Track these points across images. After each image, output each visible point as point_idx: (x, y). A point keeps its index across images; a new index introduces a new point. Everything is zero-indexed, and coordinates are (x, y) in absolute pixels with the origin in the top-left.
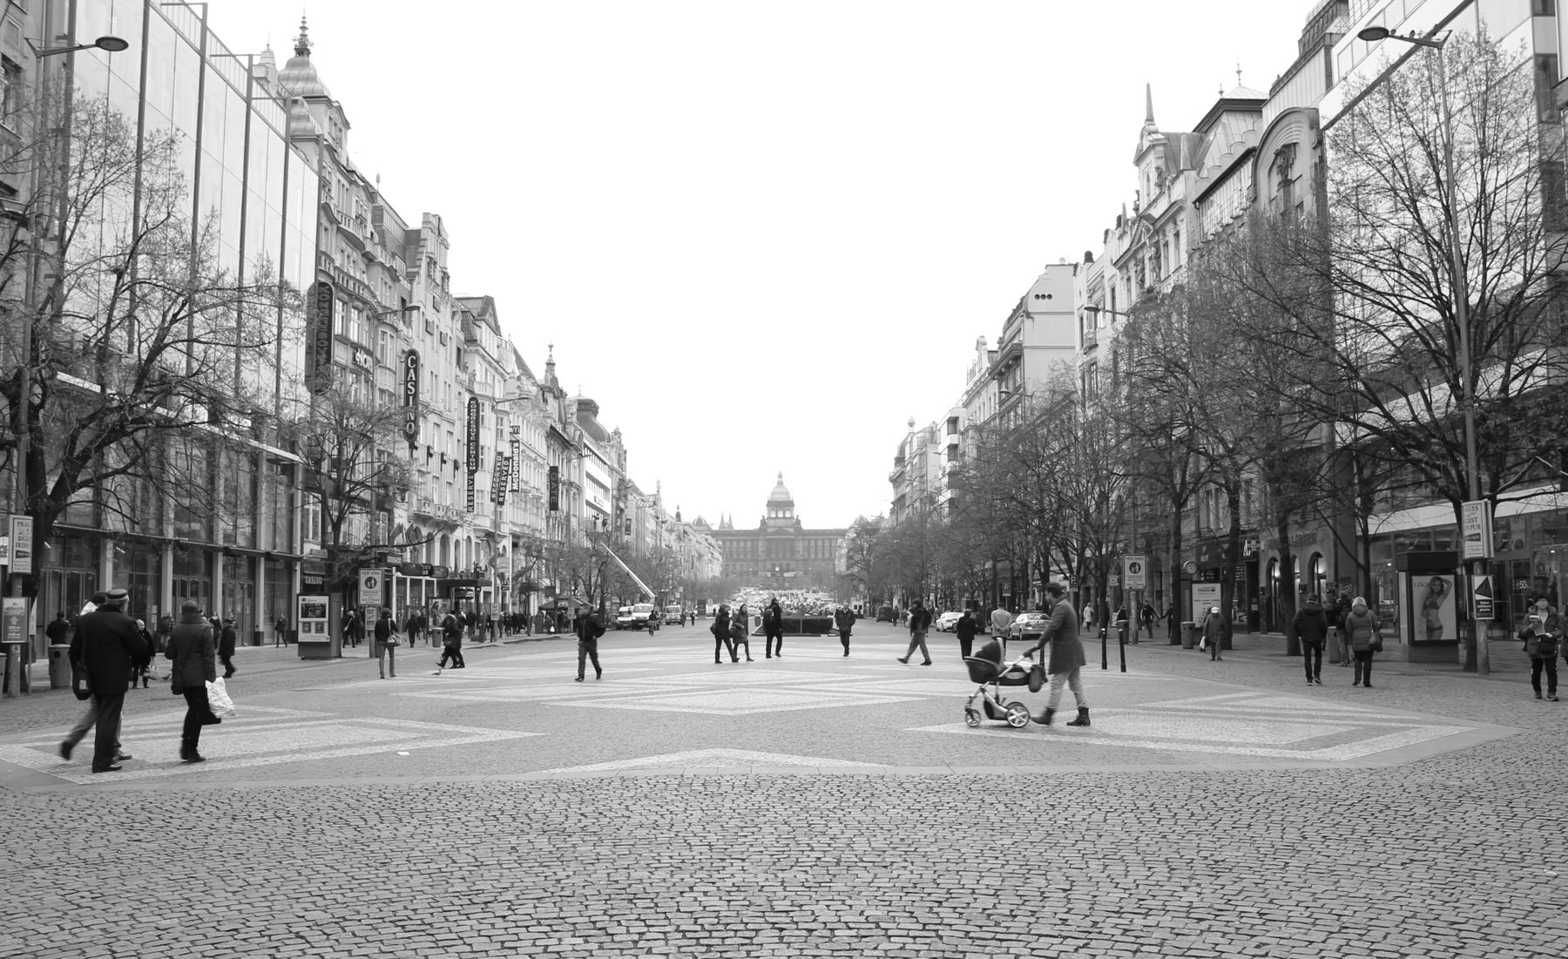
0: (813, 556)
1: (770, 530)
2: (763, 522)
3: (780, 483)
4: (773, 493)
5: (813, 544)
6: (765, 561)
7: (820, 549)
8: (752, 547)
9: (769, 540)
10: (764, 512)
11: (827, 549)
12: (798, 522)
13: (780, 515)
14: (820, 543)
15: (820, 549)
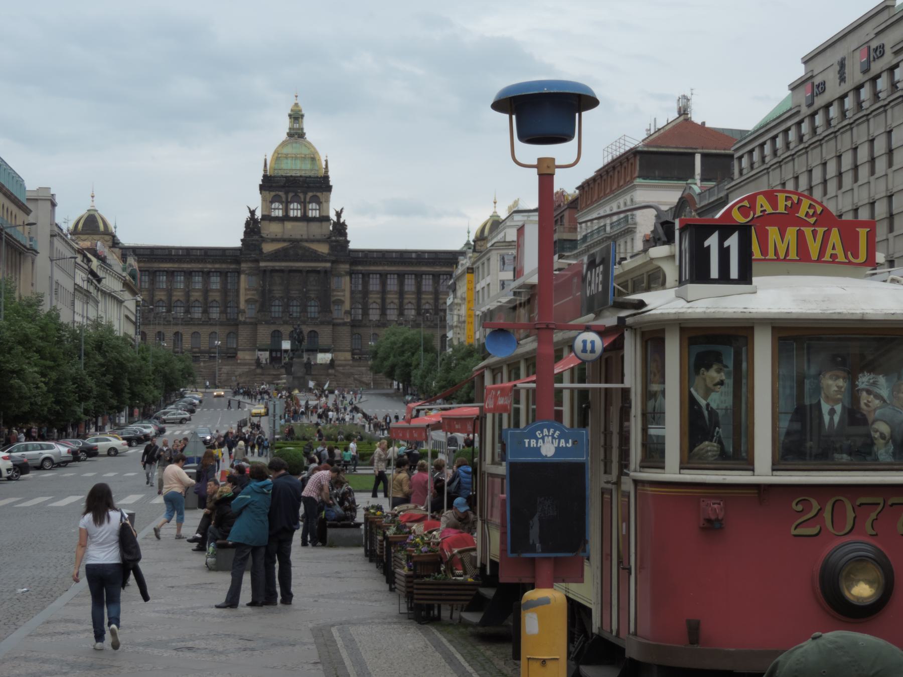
0: (374, 315)
1: (268, 248)
2: (252, 227)
3: (296, 134)
4: (278, 156)
5: (374, 284)
6: (255, 324)
7: (392, 298)
8: (225, 291)
9: (264, 273)
10: (256, 201)
11: (410, 298)
12: (340, 228)
13: (295, 211)
14: (392, 284)
15: (392, 298)
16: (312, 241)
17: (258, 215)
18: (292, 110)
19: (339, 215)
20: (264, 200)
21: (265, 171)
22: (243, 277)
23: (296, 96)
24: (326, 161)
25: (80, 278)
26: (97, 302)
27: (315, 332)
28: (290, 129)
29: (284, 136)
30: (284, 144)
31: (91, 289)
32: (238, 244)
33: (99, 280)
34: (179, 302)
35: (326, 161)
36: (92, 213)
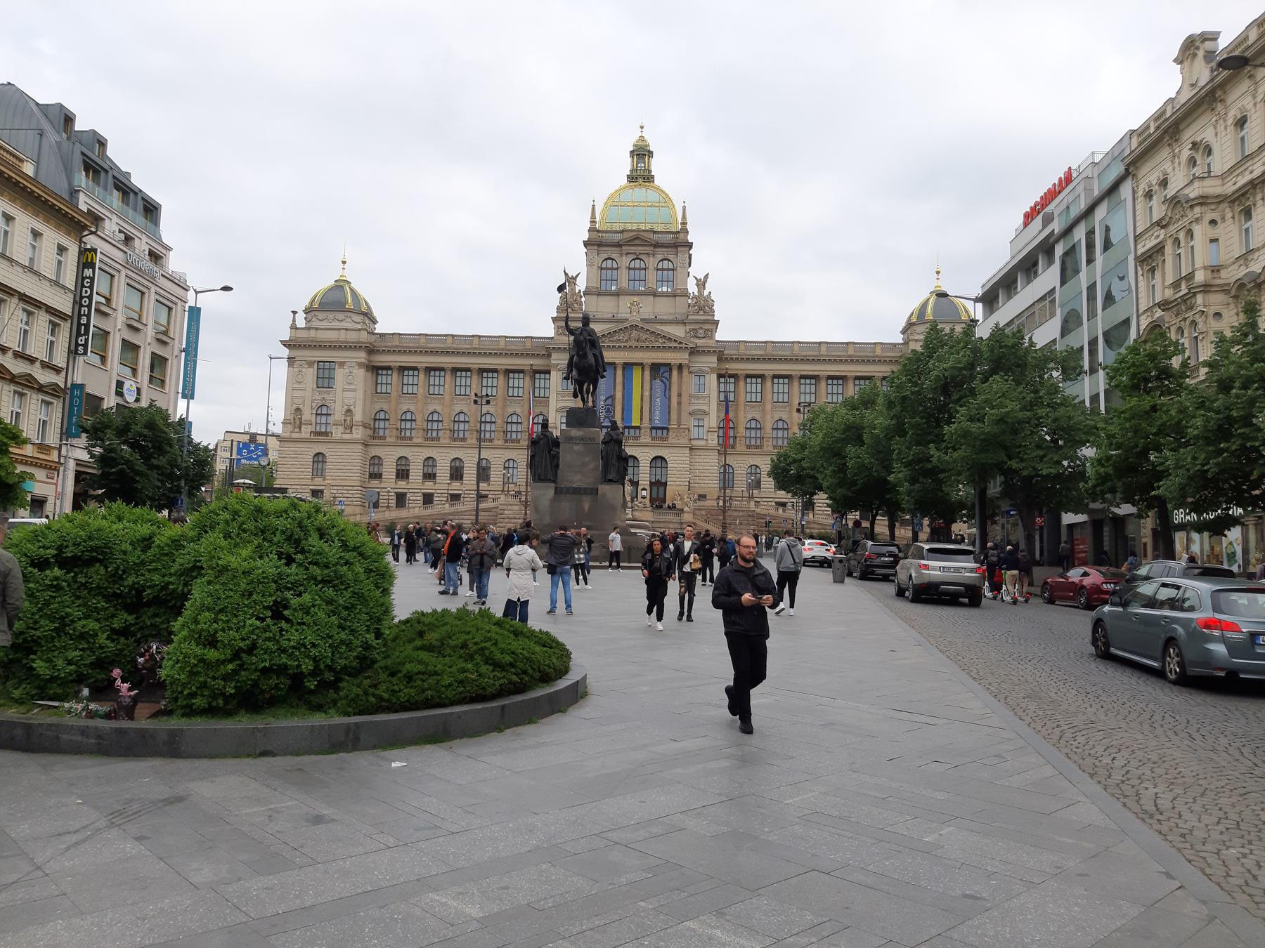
3: (641, 176)
12: (704, 306)
16: (663, 322)
17: (581, 285)
18: (635, 145)
19: (701, 284)
21: (593, 222)
23: (642, 127)
24: (684, 208)
27: (662, 458)
28: (632, 171)
29: (624, 181)
30: (622, 189)
34: (462, 415)
35: (684, 208)
36: (342, 283)
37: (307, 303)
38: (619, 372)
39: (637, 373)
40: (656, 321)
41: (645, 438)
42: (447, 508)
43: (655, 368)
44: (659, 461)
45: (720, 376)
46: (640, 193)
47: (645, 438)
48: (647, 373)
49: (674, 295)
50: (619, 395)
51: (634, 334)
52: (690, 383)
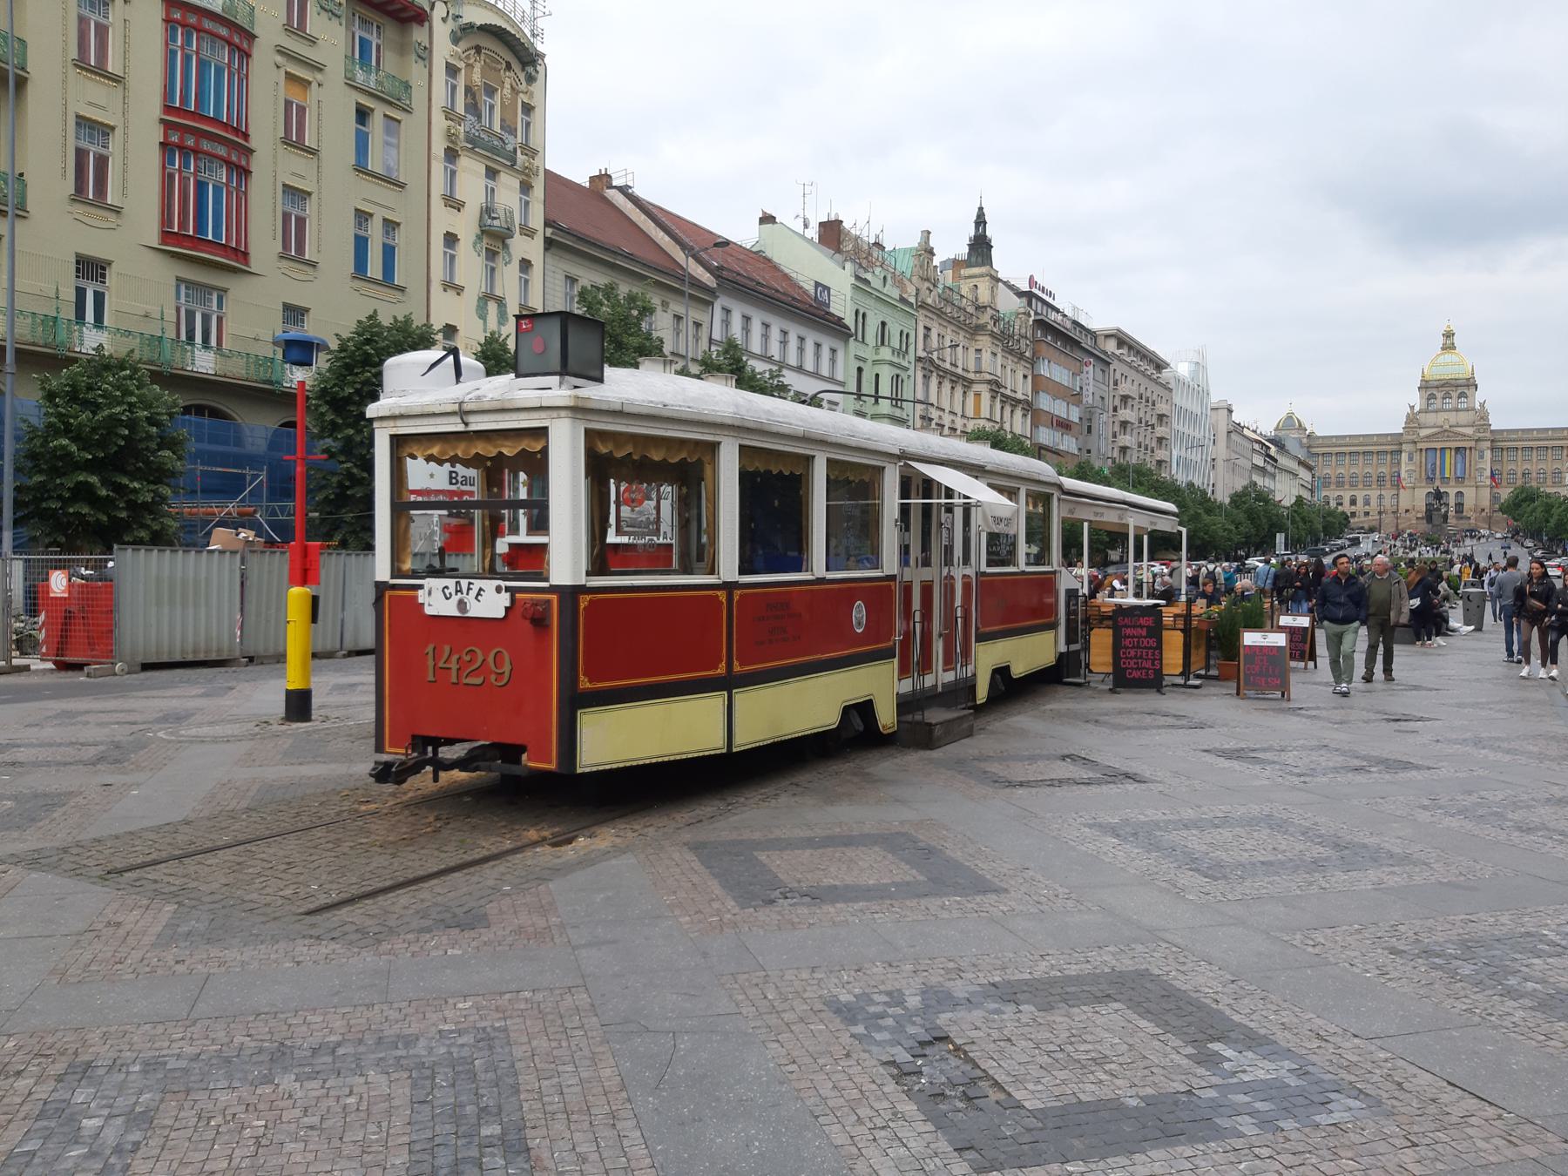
1: (1424, 433)
2: (1412, 420)
3: (1449, 347)
10: (1416, 399)
12: (1483, 416)
19: (1482, 405)
20: (1421, 398)
22: (1403, 454)
25: (1259, 461)
26: (1273, 476)
29: (1439, 351)
31: (1269, 468)
32: (1401, 431)
33: (1276, 461)
37: (1275, 425)
38: (1438, 452)
39: (1448, 452)
40: (1458, 426)
41: (1452, 483)
42: (1363, 519)
43: (1457, 449)
44: (1460, 494)
45: (1492, 449)
46: (1448, 357)
47: (1452, 483)
48: (1453, 453)
49: (1467, 410)
50: (1438, 463)
51: (1446, 434)
52: (1475, 454)
